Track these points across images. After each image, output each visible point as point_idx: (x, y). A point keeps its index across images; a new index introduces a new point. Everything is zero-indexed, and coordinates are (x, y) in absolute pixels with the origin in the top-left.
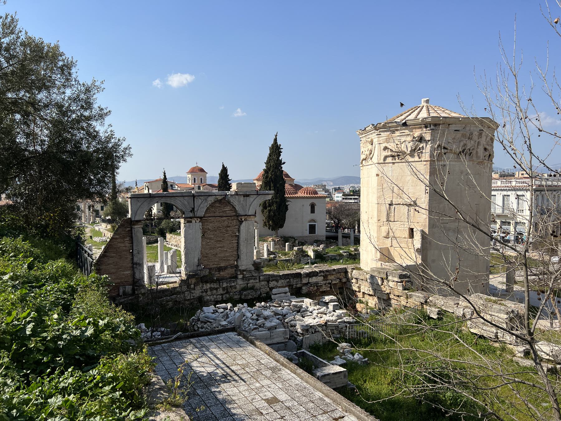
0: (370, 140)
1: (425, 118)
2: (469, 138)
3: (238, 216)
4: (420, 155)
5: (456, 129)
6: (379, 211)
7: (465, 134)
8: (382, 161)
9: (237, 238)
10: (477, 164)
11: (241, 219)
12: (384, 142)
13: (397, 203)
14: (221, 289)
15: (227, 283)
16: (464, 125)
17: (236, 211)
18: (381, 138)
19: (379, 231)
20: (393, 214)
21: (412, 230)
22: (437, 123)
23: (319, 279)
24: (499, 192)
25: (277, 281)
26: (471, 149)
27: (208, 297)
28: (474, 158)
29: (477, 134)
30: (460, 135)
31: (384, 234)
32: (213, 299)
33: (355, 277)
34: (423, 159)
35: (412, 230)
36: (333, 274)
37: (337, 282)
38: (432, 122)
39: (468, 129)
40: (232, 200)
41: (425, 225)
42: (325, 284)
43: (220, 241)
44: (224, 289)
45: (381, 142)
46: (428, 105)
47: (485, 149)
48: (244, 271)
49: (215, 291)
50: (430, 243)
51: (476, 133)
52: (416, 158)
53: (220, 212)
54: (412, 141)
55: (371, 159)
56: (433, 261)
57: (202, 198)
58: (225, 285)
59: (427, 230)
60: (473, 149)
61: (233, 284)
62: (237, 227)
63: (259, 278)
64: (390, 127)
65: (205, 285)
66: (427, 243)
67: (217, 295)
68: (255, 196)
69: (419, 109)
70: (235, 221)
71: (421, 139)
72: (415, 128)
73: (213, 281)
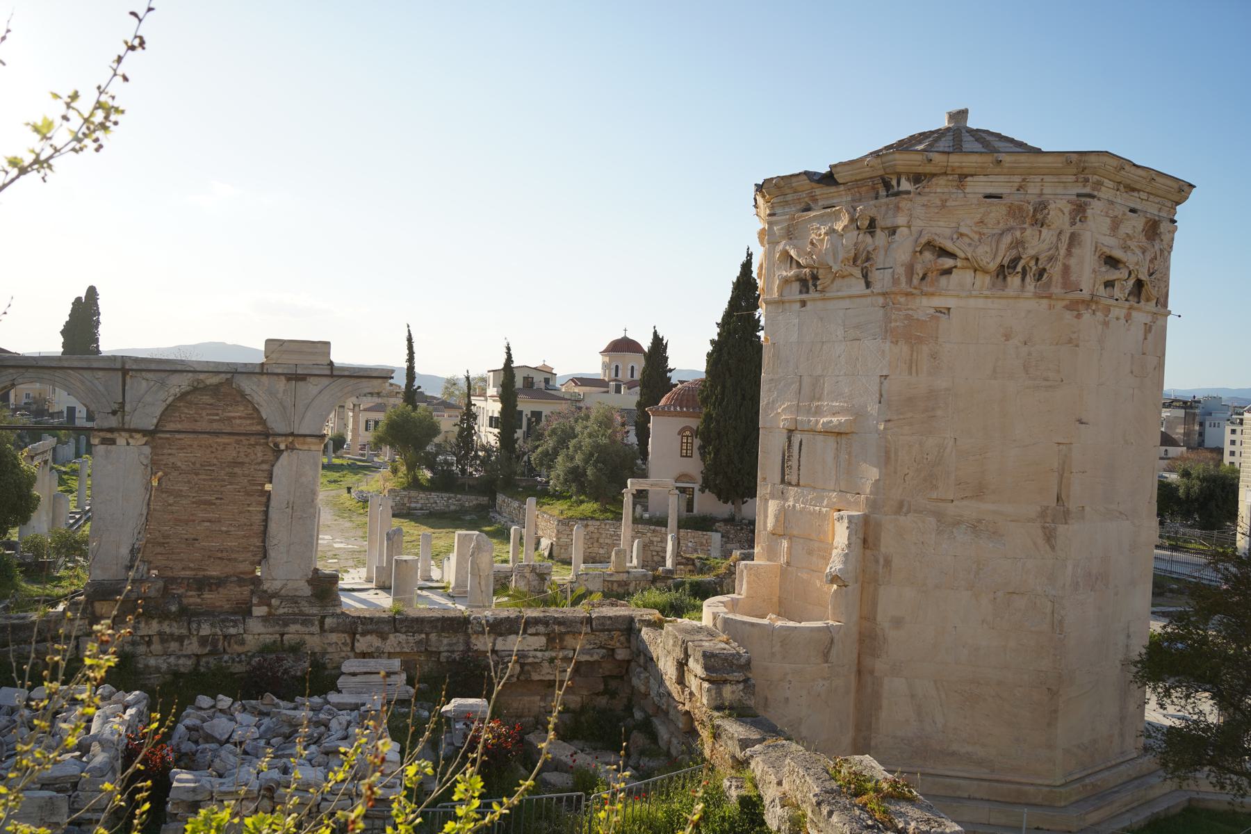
3: (267, 435)
7: (1020, 208)
9: (264, 499)
10: (1067, 308)
11: (276, 445)
14: (195, 640)
15: (213, 625)
16: (1018, 179)
17: (263, 422)
20: (794, 463)
22: (920, 170)
25: (383, 637)
26: (1043, 258)
27: (152, 662)
28: (1056, 290)
29: (1068, 208)
30: (1004, 210)
32: (164, 667)
37: (596, 657)
39: (1033, 189)
40: (247, 386)
42: (552, 660)
43: (210, 503)
44: (203, 641)
48: (275, 595)
49: (174, 646)
50: (888, 562)
53: (212, 421)
56: (898, 622)
57: (149, 375)
58: (206, 630)
60: (1050, 259)
61: (232, 631)
62: (265, 467)
63: (322, 623)
65: (142, 625)
66: (877, 562)
67: (179, 657)
68: (326, 381)
70: (259, 448)
73: (165, 616)
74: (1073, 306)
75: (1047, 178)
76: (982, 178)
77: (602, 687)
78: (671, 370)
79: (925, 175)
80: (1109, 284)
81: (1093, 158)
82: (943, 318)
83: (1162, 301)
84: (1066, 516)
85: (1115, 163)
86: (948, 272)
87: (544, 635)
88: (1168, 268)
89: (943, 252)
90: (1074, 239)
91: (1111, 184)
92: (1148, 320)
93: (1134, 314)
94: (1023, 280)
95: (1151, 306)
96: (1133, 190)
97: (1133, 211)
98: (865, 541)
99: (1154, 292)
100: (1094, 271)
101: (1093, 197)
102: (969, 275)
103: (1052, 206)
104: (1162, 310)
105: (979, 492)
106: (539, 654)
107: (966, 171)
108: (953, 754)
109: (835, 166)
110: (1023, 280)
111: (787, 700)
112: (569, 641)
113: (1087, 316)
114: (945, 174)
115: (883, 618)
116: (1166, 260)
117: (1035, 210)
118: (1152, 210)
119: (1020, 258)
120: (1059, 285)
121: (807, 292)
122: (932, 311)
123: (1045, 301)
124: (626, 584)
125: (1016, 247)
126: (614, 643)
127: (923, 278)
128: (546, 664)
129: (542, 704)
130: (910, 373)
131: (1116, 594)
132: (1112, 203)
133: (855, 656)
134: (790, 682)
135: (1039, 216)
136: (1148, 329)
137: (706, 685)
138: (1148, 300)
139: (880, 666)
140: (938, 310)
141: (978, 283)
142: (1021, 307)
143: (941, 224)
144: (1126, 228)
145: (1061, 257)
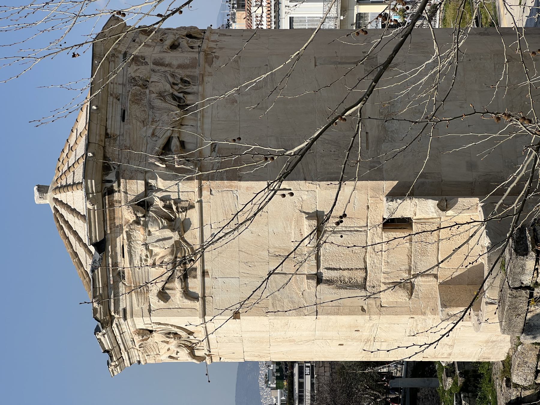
0: (137, 339)
1: (87, 194)
2: (145, 86)
4: (183, 204)
5: (119, 118)
6: (338, 310)
7: (135, 95)
8: (198, 305)
10: (210, 65)
12: (147, 300)
13: (314, 263)
16: (111, 99)
18: (136, 308)
19: (393, 310)
20: (345, 273)
21: (390, 224)
24: (283, 10)
26: (171, 80)
28: (196, 72)
29: (134, 67)
31: (401, 296)
33: (531, 377)
34: (195, 198)
35: (390, 224)
38: (99, 177)
39: (119, 90)
41: (373, 189)
45: (146, 307)
46: (52, 186)
47: (174, 47)
51: (133, 71)
52: (193, 215)
54: (145, 226)
55: (191, 333)
56: (471, 166)
59: (388, 185)
60: (173, 76)
64: (106, 285)
69: (62, 211)
71: (143, 205)
72: (113, 219)
76: (109, 122)
94: (189, 93)
103: (133, 75)
107: (103, 133)
110: (189, 93)
114: (104, 147)
119: (172, 94)
120: (193, 70)
121: (195, 269)
123: (206, 79)
125: (164, 97)
145: (172, 70)
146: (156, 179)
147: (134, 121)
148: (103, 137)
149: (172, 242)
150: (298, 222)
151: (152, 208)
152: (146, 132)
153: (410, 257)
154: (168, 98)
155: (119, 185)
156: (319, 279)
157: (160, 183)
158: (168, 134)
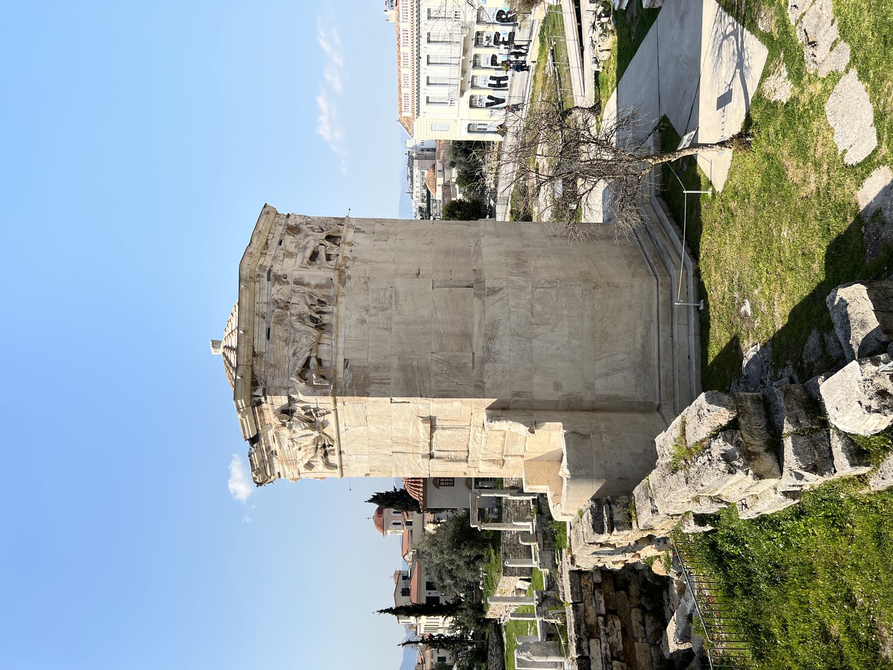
4: (321, 411)
5: (264, 336)
7: (276, 317)
10: (344, 284)
16: (257, 319)
20: (452, 453)
22: (249, 383)
23: (597, 650)
26: (309, 302)
29: (277, 286)
34: (331, 407)
36: (585, 610)
37: (602, 599)
38: (248, 395)
39: (264, 309)
41: (476, 403)
42: (607, 635)
46: (223, 344)
50: (517, 394)
52: (331, 418)
54: (290, 428)
56: (557, 386)
60: (311, 297)
64: (262, 461)
74: (343, 282)
75: (257, 300)
77: (622, 592)
78: (395, 489)
79: (253, 378)
80: (328, 258)
81: (244, 273)
82: (351, 363)
83: (341, 221)
84: (480, 282)
85: (247, 258)
86: (320, 361)
87: (589, 640)
88: (319, 218)
89: (306, 365)
90: (299, 282)
91: (262, 259)
92: (352, 230)
93: (348, 240)
94: (325, 313)
95: (344, 229)
96: (267, 243)
97: (280, 243)
98: (503, 409)
99: (334, 228)
100: (319, 268)
101: (270, 270)
102: (323, 348)
103: (276, 297)
104: (346, 222)
105: (466, 336)
106: (603, 645)
107: (251, 353)
108: (643, 347)
109: (245, 437)
110: (325, 313)
111: (618, 464)
112: (591, 620)
113: (349, 272)
114: (252, 366)
115: (556, 396)
116: (313, 219)
117: (279, 308)
118: (280, 229)
122: (347, 371)
123: (340, 299)
124: (545, 533)
126: (590, 586)
127: (323, 377)
128: (611, 639)
129: (640, 640)
130: (389, 383)
131: (528, 246)
132: (275, 258)
133: (583, 414)
134: (606, 462)
135: (282, 305)
136: (358, 230)
137: (615, 532)
138: (339, 231)
139: (588, 397)
140: (346, 367)
141: (328, 341)
142: (345, 314)
143: (286, 367)
144: (291, 248)
145: (310, 290)
146: (297, 393)
147: (278, 341)
148: (250, 357)
149: (313, 437)
150: (414, 422)
151: (295, 414)
152: (288, 351)
153: (503, 446)
154: (306, 320)
155: (266, 399)
156: (431, 456)
157: (301, 397)
158: (307, 354)
